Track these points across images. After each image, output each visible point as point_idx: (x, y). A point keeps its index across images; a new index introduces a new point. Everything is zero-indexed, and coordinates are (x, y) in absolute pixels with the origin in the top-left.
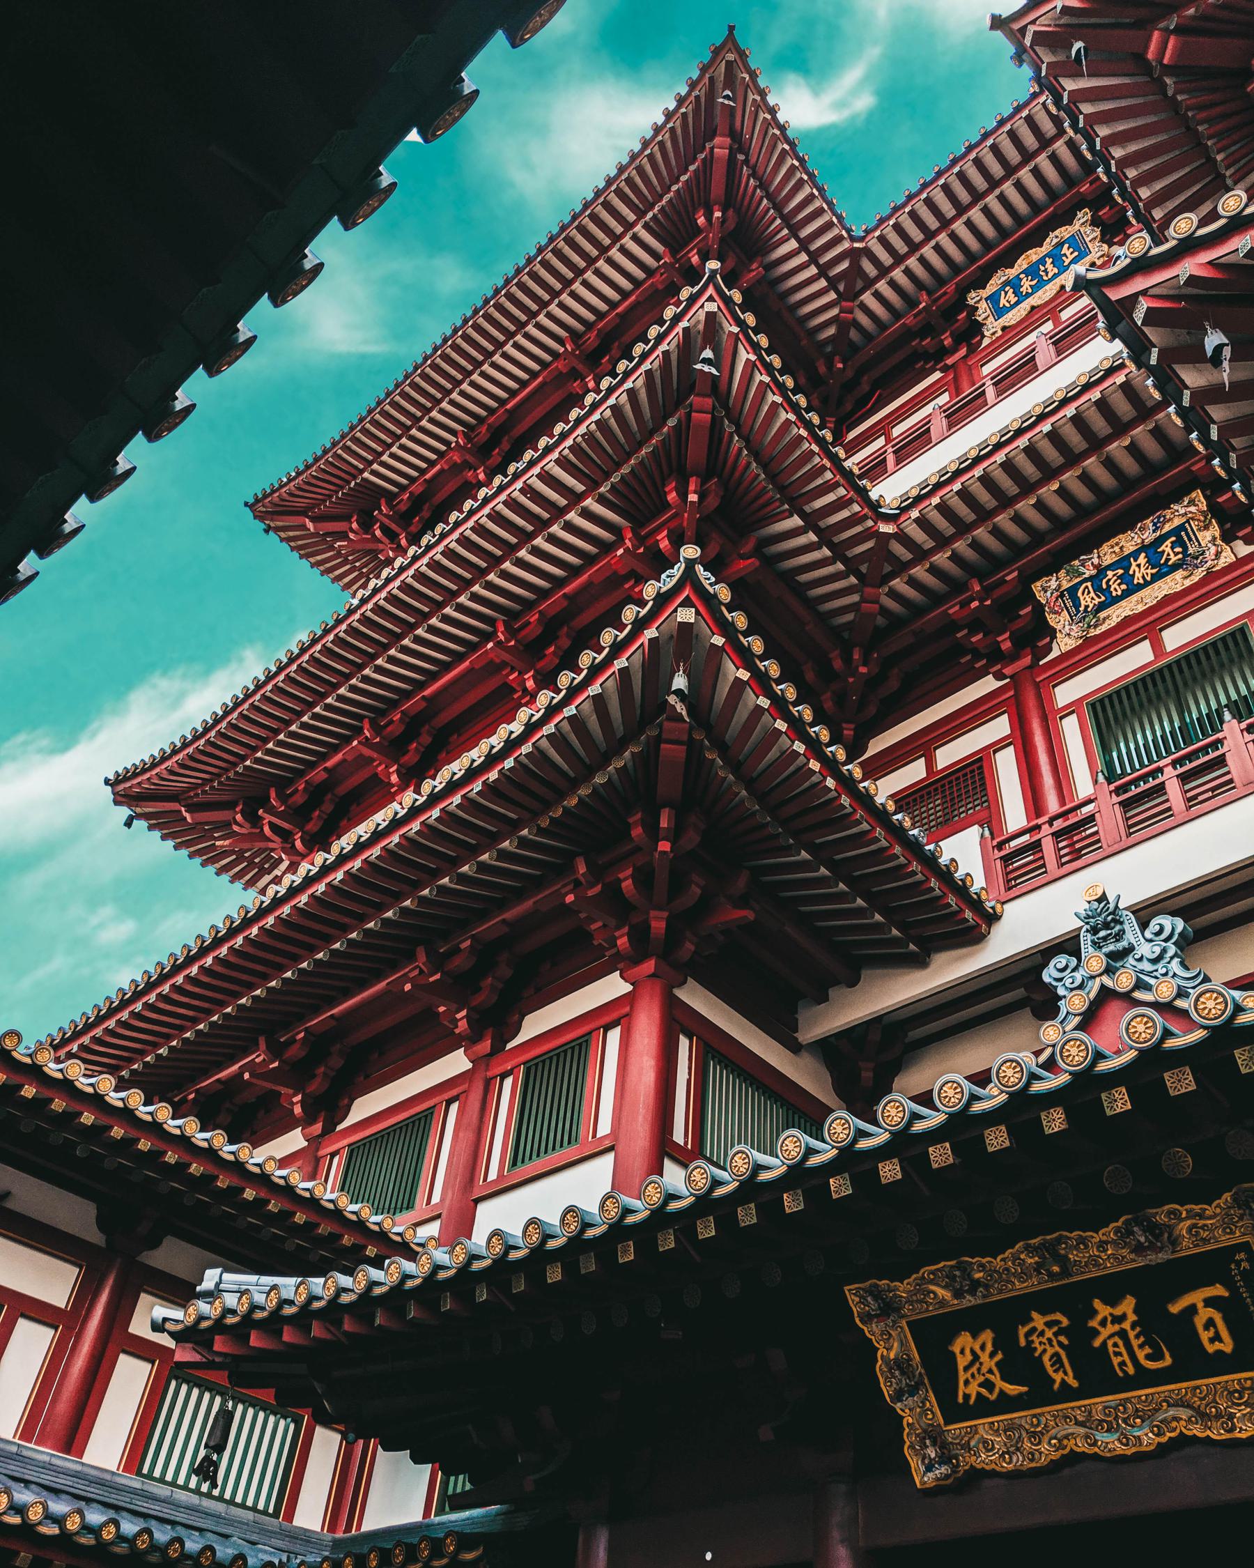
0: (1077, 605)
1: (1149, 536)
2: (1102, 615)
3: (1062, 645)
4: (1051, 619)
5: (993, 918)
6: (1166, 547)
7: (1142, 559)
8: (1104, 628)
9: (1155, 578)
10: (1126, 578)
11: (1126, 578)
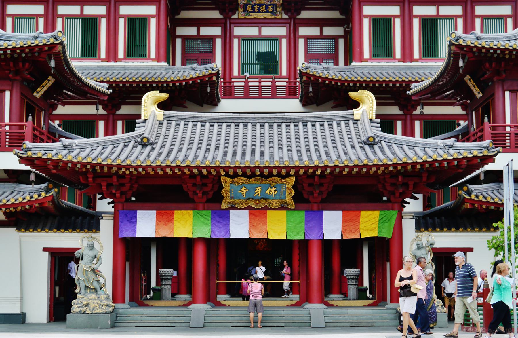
0: (246, 8)
1: (268, 3)
2: (251, 14)
3: (240, 15)
4: (239, 9)
5: (219, 101)
6: (270, 7)
7: (264, 7)
8: (250, 17)
9: (265, 12)
10: (259, 9)
11: (259, 9)
